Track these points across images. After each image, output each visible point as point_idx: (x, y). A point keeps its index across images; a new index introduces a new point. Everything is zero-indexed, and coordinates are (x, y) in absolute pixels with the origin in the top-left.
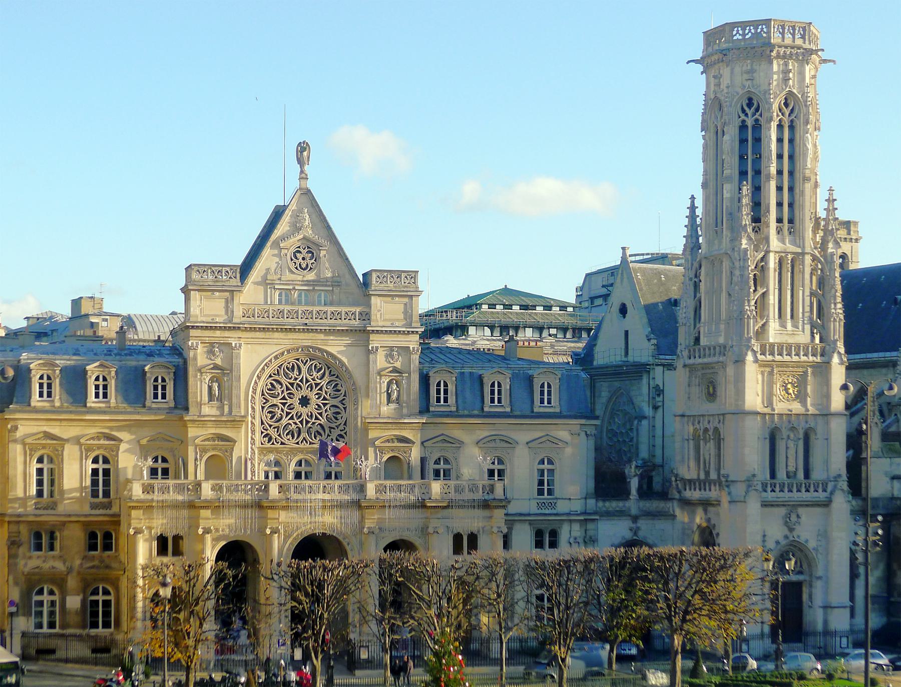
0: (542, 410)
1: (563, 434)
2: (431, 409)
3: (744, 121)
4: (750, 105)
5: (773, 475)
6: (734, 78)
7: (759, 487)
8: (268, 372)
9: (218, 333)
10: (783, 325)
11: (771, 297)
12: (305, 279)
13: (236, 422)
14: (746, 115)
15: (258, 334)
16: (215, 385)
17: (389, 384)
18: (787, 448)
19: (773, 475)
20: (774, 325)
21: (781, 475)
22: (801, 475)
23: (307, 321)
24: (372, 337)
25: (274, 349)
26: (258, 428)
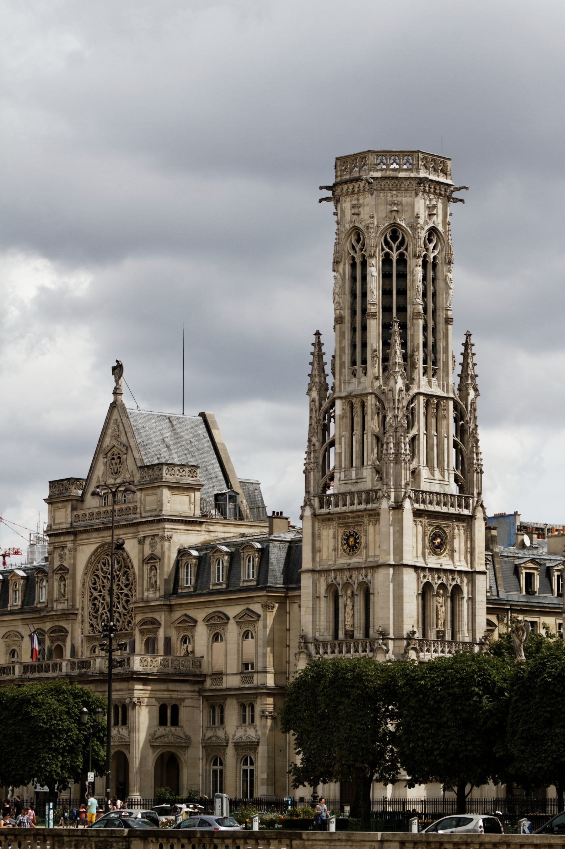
0: (246, 584)
1: (257, 608)
2: (180, 591)
3: (387, 255)
4: (394, 237)
5: (336, 636)
6: (373, 212)
7: (312, 648)
8: (91, 568)
9: (62, 539)
10: (432, 469)
11: (421, 440)
12: (116, 482)
13: (70, 614)
14: (391, 248)
15: (85, 536)
16: (62, 584)
17: (151, 569)
18: (345, 606)
19: (336, 636)
20: (425, 473)
21: (341, 635)
22: (359, 634)
23: (105, 520)
24: (141, 528)
25: (93, 547)
26: (87, 619)
